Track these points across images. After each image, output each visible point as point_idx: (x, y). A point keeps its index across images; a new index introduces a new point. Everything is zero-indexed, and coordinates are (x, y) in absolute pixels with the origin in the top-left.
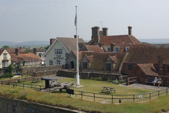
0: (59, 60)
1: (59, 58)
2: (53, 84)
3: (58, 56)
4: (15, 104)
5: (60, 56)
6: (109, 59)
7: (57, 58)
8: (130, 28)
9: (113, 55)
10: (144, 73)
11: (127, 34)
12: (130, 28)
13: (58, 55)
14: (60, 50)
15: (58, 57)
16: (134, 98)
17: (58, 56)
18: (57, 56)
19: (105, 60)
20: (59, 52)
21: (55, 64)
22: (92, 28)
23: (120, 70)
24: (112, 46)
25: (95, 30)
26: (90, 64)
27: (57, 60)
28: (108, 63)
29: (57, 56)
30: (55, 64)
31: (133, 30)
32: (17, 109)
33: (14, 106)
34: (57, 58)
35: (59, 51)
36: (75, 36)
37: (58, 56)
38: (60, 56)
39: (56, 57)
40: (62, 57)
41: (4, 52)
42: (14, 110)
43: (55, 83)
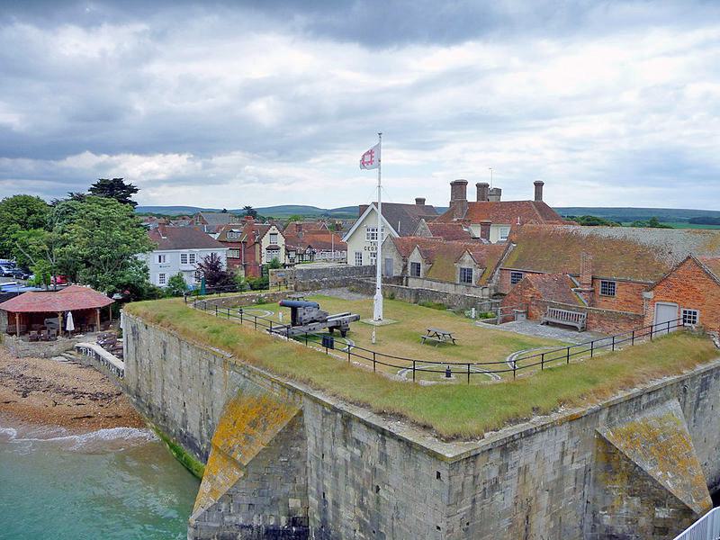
2: (307, 317)
8: (539, 186)
12: (539, 186)
16: (469, 373)
25: (458, 187)
28: (465, 266)
32: (215, 372)
41: (271, 231)
42: (211, 374)
43: (314, 314)
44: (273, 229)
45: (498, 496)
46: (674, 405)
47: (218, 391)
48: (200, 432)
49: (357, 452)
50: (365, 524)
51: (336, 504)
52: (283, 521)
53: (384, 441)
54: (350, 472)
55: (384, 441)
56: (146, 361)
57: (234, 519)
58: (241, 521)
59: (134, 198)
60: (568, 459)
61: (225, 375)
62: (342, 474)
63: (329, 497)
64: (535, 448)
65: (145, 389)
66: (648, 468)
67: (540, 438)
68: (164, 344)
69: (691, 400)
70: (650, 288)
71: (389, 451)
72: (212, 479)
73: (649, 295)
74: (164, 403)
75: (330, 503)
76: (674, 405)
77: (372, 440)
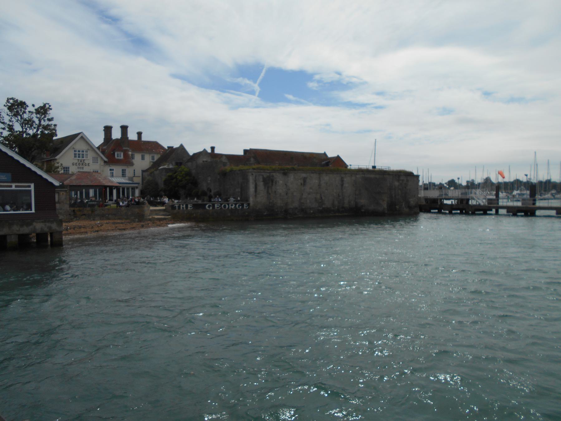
0: (82, 166)
1: (82, 164)
3: (81, 161)
5: (84, 160)
7: (77, 164)
13: (79, 158)
14: (83, 151)
15: (81, 163)
17: (81, 161)
18: (78, 160)
20: (86, 154)
27: (78, 168)
29: (78, 160)
33: (342, 178)
34: (77, 164)
37: (79, 161)
38: (84, 160)
39: (76, 161)
40: (86, 162)
63: (393, 196)
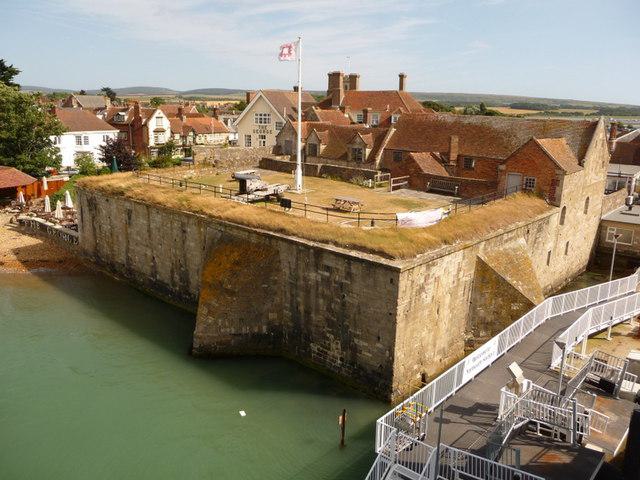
4: (186, 221)
6: (358, 140)
9: (366, 132)
10: (421, 170)
11: (397, 88)
12: (402, 77)
19: (351, 141)
21: (256, 142)
22: (330, 75)
23: (378, 161)
24: (366, 112)
25: (334, 77)
26: (322, 147)
28: (356, 147)
30: (256, 142)
31: (406, 80)
33: (183, 225)
35: (263, 117)
36: (296, 89)
41: (156, 114)
42: (184, 232)
44: (159, 113)
45: (424, 295)
46: (522, 241)
47: (192, 244)
48: (172, 278)
49: (327, 274)
50: (332, 321)
51: (308, 313)
52: (264, 328)
53: (349, 264)
54: (320, 288)
55: (349, 264)
56: (106, 227)
57: (228, 330)
58: (233, 331)
59: (15, 79)
60: (462, 273)
61: (200, 233)
62: (313, 291)
63: (302, 308)
64: (444, 265)
65: (106, 250)
66: (508, 279)
67: (447, 259)
68: (129, 213)
69: (531, 238)
70: (503, 162)
71: (354, 271)
72: (208, 305)
73: (503, 167)
74: (128, 259)
75: (303, 313)
76: (522, 241)
77: (341, 266)
